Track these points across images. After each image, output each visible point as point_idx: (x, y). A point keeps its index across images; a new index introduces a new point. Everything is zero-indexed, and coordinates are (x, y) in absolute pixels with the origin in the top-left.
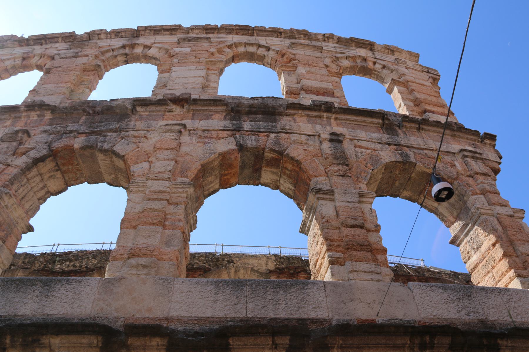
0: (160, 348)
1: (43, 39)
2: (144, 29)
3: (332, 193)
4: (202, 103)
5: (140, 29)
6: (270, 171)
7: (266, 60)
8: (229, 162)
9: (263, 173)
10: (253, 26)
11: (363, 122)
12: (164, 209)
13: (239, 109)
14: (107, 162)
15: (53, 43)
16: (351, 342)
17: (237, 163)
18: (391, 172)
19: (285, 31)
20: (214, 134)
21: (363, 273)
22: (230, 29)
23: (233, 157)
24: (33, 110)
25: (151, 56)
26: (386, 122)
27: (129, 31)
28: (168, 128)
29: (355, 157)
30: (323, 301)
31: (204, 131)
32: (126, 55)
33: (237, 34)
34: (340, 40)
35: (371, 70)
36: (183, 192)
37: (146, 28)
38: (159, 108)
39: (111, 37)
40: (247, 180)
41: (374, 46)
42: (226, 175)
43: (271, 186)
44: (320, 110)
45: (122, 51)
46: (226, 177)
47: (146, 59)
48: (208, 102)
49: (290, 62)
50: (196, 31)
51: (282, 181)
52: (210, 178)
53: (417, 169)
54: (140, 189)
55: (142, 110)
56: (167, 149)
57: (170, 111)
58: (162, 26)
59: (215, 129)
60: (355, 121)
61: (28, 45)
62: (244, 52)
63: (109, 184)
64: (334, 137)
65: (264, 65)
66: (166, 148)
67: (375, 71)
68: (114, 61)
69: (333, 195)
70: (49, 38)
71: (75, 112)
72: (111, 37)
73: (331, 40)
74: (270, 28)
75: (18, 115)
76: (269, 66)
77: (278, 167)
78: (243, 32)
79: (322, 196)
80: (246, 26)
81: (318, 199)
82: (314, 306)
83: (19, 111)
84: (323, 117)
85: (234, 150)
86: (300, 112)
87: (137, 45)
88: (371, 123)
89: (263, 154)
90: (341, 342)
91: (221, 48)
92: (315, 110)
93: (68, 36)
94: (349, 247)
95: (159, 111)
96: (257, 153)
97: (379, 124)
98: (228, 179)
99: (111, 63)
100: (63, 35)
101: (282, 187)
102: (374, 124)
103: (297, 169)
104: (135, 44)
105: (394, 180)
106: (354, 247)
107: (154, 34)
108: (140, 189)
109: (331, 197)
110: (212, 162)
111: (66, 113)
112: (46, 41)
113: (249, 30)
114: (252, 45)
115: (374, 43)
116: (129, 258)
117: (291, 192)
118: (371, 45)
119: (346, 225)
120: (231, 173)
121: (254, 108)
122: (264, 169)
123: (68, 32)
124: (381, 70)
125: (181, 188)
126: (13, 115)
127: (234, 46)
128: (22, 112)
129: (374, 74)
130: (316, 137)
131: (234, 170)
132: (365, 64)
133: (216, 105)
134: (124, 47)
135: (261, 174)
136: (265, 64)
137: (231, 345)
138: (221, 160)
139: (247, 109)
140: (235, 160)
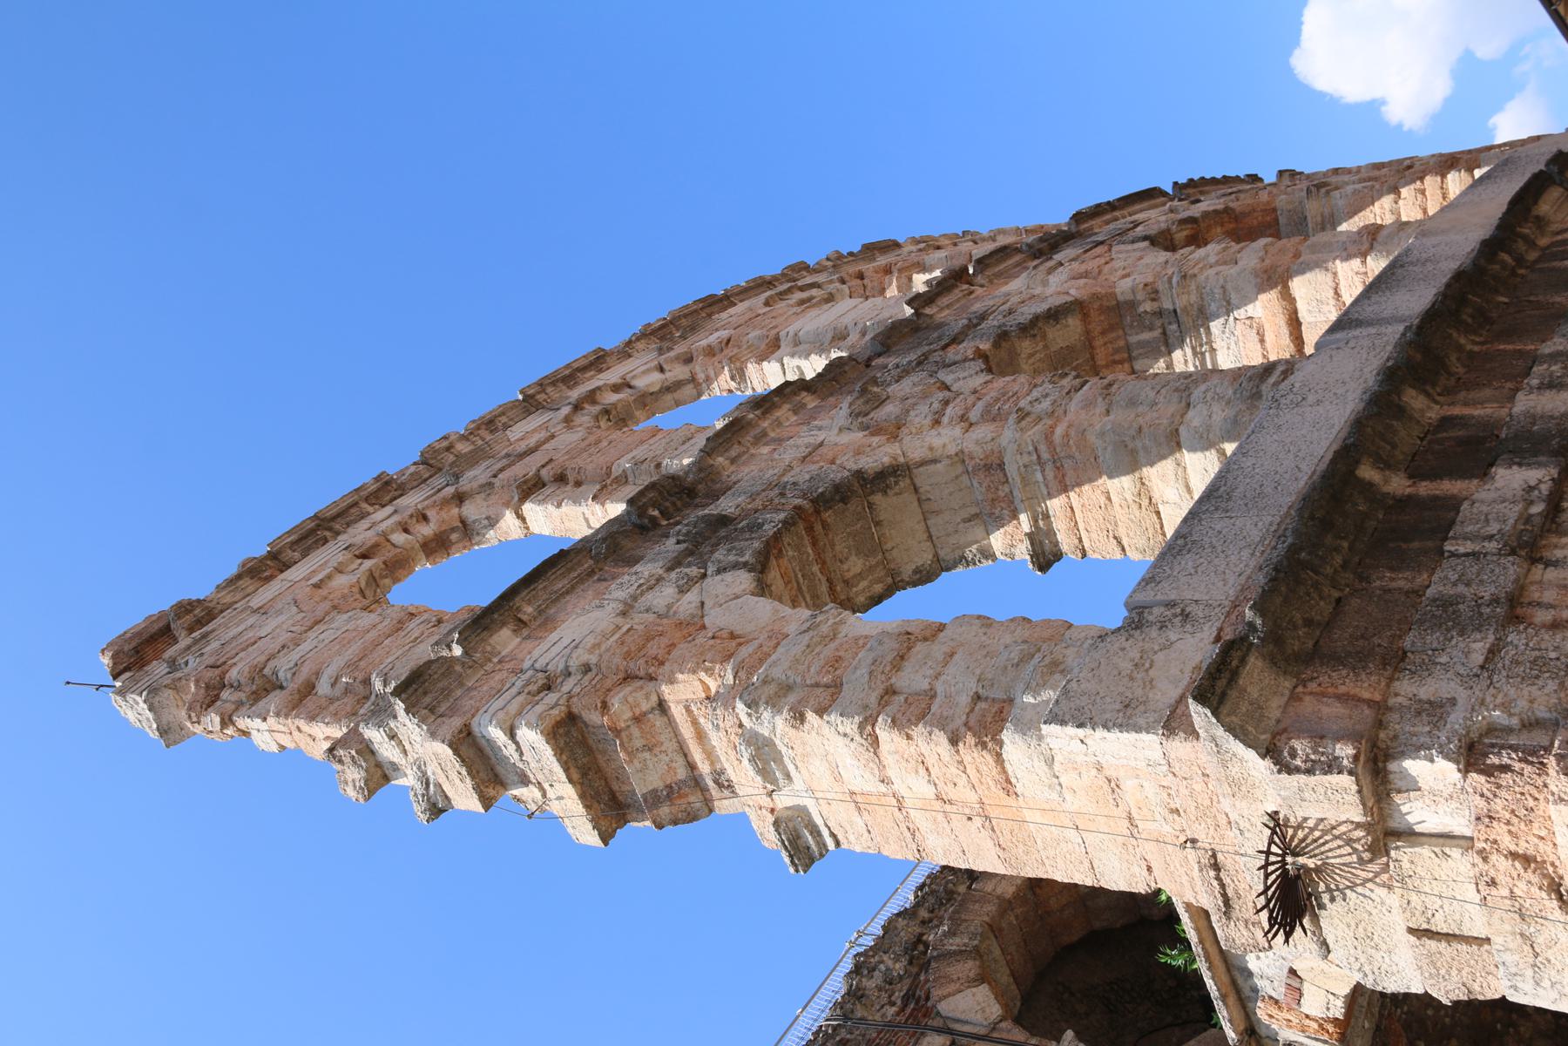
2: (538, 388)
5: (531, 392)
22: (691, 313)
37: (541, 385)
70: (334, 518)
78: (715, 308)
81: (1328, 192)
93: (379, 490)
95: (958, 300)
100: (364, 493)
111: (834, 379)
112: (330, 529)
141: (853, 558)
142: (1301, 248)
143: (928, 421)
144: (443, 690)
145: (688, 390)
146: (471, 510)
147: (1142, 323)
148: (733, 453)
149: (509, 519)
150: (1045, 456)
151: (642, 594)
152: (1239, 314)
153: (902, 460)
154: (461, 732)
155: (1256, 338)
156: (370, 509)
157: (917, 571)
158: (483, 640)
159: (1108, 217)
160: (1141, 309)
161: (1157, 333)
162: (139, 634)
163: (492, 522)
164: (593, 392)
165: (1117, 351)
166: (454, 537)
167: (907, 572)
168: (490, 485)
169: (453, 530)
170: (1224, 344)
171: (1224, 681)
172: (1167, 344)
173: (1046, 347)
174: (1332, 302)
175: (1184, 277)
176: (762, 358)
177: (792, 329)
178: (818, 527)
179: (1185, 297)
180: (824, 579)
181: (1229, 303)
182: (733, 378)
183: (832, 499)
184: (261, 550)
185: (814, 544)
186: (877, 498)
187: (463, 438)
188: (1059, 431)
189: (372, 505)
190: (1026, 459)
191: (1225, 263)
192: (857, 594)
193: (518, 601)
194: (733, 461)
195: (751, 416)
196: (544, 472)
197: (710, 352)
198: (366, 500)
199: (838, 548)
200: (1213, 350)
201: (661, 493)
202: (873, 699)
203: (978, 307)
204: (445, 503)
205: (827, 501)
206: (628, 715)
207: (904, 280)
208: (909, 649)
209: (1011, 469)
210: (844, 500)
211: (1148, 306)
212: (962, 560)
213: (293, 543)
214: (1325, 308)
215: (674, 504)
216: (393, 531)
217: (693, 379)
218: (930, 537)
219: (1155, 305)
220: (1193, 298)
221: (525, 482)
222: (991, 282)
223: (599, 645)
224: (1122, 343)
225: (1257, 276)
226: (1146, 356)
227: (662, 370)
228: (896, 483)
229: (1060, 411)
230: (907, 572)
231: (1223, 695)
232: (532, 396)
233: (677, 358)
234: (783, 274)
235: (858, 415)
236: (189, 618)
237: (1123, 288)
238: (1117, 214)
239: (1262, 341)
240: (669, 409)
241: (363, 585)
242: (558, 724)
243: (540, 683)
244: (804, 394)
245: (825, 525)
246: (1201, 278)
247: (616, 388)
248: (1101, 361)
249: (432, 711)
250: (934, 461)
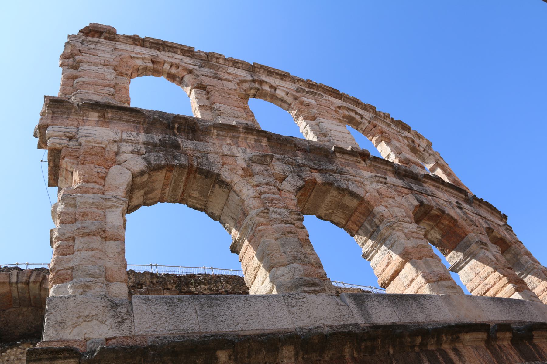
1: (161, 44)
2: (259, 67)
7: (360, 126)
15: (172, 52)
19: (362, 104)
22: (326, 89)
24: (252, 134)
28: (378, 178)
33: (330, 95)
37: (261, 67)
38: (351, 158)
39: (229, 65)
48: (382, 161)
50: (301, 83)
53: (494, 234)
57: (359, 163)
58: (275, 69)
61: (143, 46)
63: (319, 217)
65: (357, 129)
67: (420, 152)
70: (167, 46)
71: (289, 145)
72: (229, 65)
75: (236, 134)
76: (362, 132)
78: (334, 95)
81: (482, 248)
83: (238, 131)
93: (187, 50)
95: (352, 161)
100: (182, 48)
101: (429, 236)
103: (452, 225)
111: (280, 144)
112: (164, 48)
113: (339, 94)
117: (436, 241)
123: (188, 45)
126: (231, 134)
128: (240, 133)
129: (418, 154)
136: (359, 129)
141: (197, 192)
142: (424, 258)
143: (255, 183)
144: (62, 111)
145: (286, 106)
146: (188, 78)
147: (372, 223)
148: (221, 133)
149: (189, 88)
150: (254, 229)
151: (127, 142)
152: (391, 253)
153: (233, 184)
154: (45, 125)
155: (386, 264)
156: (179, 52)
157: (212, 213)
158: (88, 110)
159: (437, 184)
160: (375, 220)
161: (372, 230)
162: (97, 27)
163: (187, 86)
164: (264, 81)
165: (359, 221)
166: (178, 79)
167: (210, 211)
168: (198, 76)
169: (179, 77)
170: (380, 254)
171: (47, 356)
172: (371, 236)
173: (341, 199)
174: (409, 281)
175: (391, 226)
176: (305, 119)
177: (321, 120)
178: (192, 176)
179: (385, 231)
180: (182, 189)
181: (392, 246)
182: (295, 115)
183: (203, 173)
184: (142, 36)
185: (187, 178)
186: (217, 186)
187: (225, 59)
188: (261, 227)
189: (181, 52)
190: (250, 223)
191: (406, 236)
192: (190, 201)
193: (109, 110)
194: (218, 135)
195: (241, 130)
196: (208, 87)
197: (302, 103)
198: (181, 50)
199: (194, 186)
200: (377, 252)
201: (186, 123)
202: (68, 235)
203: (346, 169)
204: (185, 69)
205: (201, 172)
206: (65, 166)
207: (380, 140)
208: (94, 235)
209: (247, 220)
210: (206, 177)
211: (377, 221)
212: (223, 223)
213: (151, 42)
214: (406, 280)
215: (185, 129)
216: (168, 63)
217: (290, 105)
218: (223, 210)
219: (379, 223)
220: (387, 234)
221: (202, 85)
222: (370, 166)
223: (90, 142)
224: (362, 221)
225: (403, 250)
226: (364, 232)
227: (287, 94)
228: (225, 188)
229: (272, 223)
230: (210, 211)
231: (40, 360)
232: (255, 67)
233: (294, 95)
234: (366, 105)
235: (251, 160)
236: (108, 35)
237: (379, 209)
238: (441, 186)
239: (387, 266)
240: (277, 105)
241: (141, 68)
242: (55, 149)
243: (71, 135)
244: (266, 139)
245: (195, 177)
246: (394, 232)
247: (271, 86)
248: (353, 218)
249: (53, 113)
250: (238, 195)
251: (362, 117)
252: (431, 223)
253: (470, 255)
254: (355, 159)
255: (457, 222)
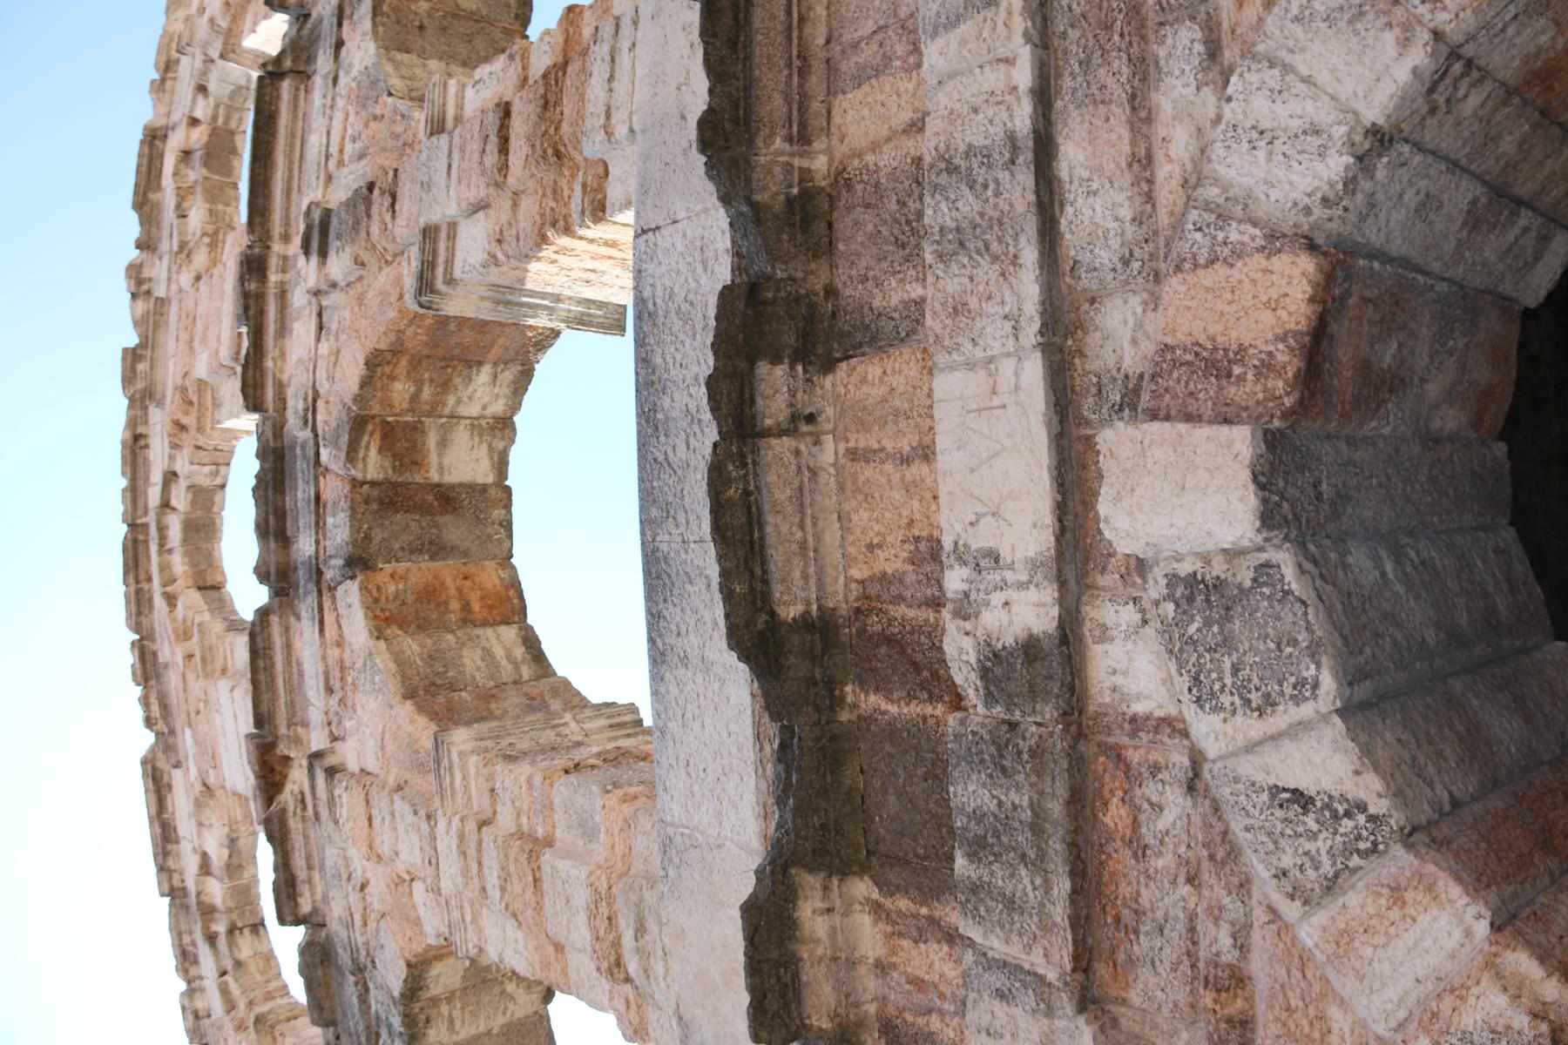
0: (838, 903)
2: (165, 875)
3: (429, 234)
4: (265, 697)
5: (166, 888)
6: (441, 455)
7: (206, 482)
8: (410, 598)
9: (453, 477)
10: (125, 528)
11: (292, 145)
12: (500, 840)
13: (273, 570)
14: (456, 1013)
16: (778, 100)
17: (419, 570)
18: (421, 28)
19: (132, 423)
20: (334, 653)
21: (615, 85)
22: (138, 601)
23: (392, 588)
25: (226, 852)
26: (288, 63)
27: (177, 920)
29: (364, 162)
30: (684, 236)
31: (330, 690)
32: (232, 930)
34: (146, 244)
35: (214, 132)
36: (464, 768)
37: (162, 869)
38: (297, 839)
40: (489, 530)
41: (155, 130)
42: (466, 607)
43: (501, 445)
44: (260, 297)
45: (222, 942)
46: (476, 606)
47: (240, 866)
48: (262, 677)
49: (191, 403)
51: (473, 410)
52: (467, 661)
54: (468, 918)
55: (307, 894)
56: (370, 819)
57: (303, 801)
59: (320, 653)
60: (291, 171)
62: (185, 554)
64: (315, 244)
65: (223, 486)
66: (366, 823)
67: (215, 118)
68: (253, 969)
69: (437, 229)
73: (146, 274)
74: (123, 474)
76: (223, 469)
77: (416, 429)
78: (142, 560)
79: (440, 270)
80: (125, 550)
81: (450, 281)
82: (700, 270)
84: (282, 283)
85: (364, 588)
86: (269, 364)
87: (203, 898)
88: (295, 117)
89: (373, 484)
90: (778, 142)
91: (175, 630)
92: (262, 312)
94: (550, 151)
95: (306, 837)
96: (375, 506)
97: (297, 89)
98: (483, 598)
99: (259, 978)
101: (498, 408)
102: (296, 106)
104: (199, 903)
105: (455, 16)
106: (552, 131)
107: (177, 842)
108: (468, 918)
109: (443, 235)
110: (401, 661)
113: (135, 541)
114: (162, 529)
115: (146, 128)
116: (628, 979)
117: (508, 375)
118: (154, 137)
119: (500, 170)
120: (459, 590)
121: (266, 521)
122: (434, 476)
124: (211, 100)
125: (452, 776)
127: (169, 589)
129: (227, 119)
130: (324, 303)
131: (449, 580)
132: (198, 154)
133: (269, 648)
134: (211, 939)
135: (461, 485)
136: (218, 481)
137: (807, 612)
138: (401, 627)
139: (273, 545)
140: (404, 578)
234: (132, 401)
251: (171, 476)
252: (432, 440)
253: (508, 303)
254: (294, 824)
255: (377, 353)
